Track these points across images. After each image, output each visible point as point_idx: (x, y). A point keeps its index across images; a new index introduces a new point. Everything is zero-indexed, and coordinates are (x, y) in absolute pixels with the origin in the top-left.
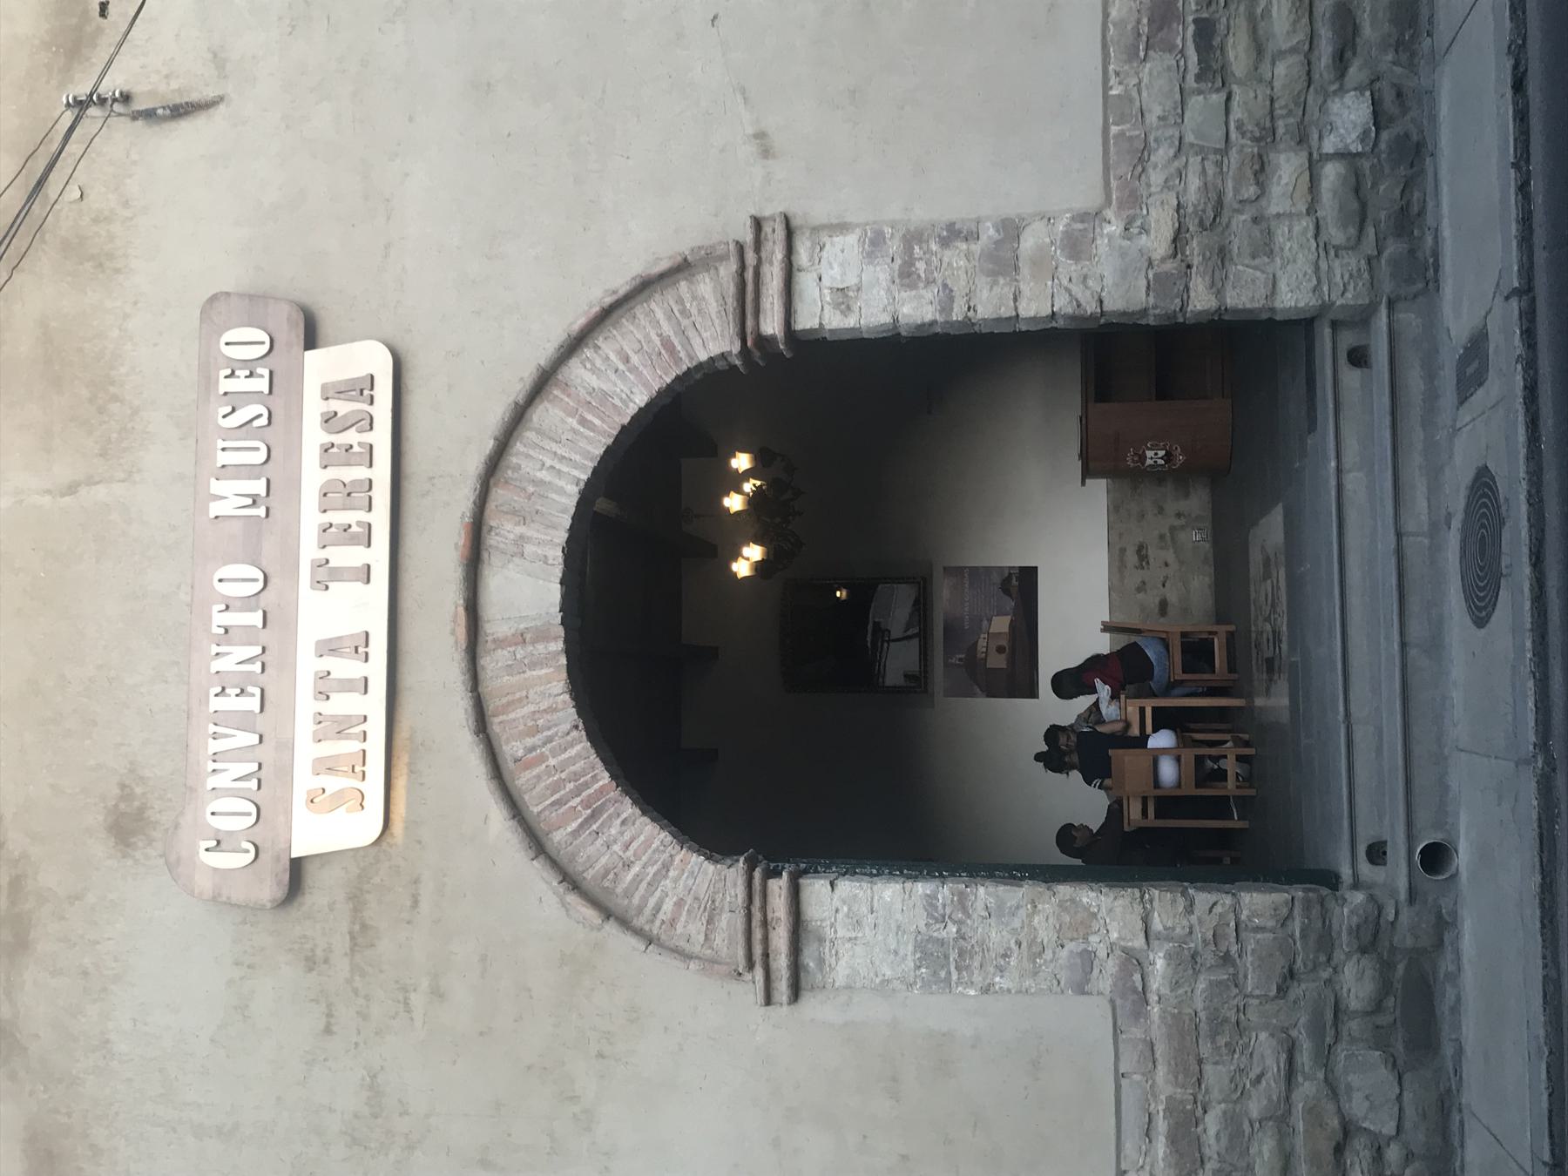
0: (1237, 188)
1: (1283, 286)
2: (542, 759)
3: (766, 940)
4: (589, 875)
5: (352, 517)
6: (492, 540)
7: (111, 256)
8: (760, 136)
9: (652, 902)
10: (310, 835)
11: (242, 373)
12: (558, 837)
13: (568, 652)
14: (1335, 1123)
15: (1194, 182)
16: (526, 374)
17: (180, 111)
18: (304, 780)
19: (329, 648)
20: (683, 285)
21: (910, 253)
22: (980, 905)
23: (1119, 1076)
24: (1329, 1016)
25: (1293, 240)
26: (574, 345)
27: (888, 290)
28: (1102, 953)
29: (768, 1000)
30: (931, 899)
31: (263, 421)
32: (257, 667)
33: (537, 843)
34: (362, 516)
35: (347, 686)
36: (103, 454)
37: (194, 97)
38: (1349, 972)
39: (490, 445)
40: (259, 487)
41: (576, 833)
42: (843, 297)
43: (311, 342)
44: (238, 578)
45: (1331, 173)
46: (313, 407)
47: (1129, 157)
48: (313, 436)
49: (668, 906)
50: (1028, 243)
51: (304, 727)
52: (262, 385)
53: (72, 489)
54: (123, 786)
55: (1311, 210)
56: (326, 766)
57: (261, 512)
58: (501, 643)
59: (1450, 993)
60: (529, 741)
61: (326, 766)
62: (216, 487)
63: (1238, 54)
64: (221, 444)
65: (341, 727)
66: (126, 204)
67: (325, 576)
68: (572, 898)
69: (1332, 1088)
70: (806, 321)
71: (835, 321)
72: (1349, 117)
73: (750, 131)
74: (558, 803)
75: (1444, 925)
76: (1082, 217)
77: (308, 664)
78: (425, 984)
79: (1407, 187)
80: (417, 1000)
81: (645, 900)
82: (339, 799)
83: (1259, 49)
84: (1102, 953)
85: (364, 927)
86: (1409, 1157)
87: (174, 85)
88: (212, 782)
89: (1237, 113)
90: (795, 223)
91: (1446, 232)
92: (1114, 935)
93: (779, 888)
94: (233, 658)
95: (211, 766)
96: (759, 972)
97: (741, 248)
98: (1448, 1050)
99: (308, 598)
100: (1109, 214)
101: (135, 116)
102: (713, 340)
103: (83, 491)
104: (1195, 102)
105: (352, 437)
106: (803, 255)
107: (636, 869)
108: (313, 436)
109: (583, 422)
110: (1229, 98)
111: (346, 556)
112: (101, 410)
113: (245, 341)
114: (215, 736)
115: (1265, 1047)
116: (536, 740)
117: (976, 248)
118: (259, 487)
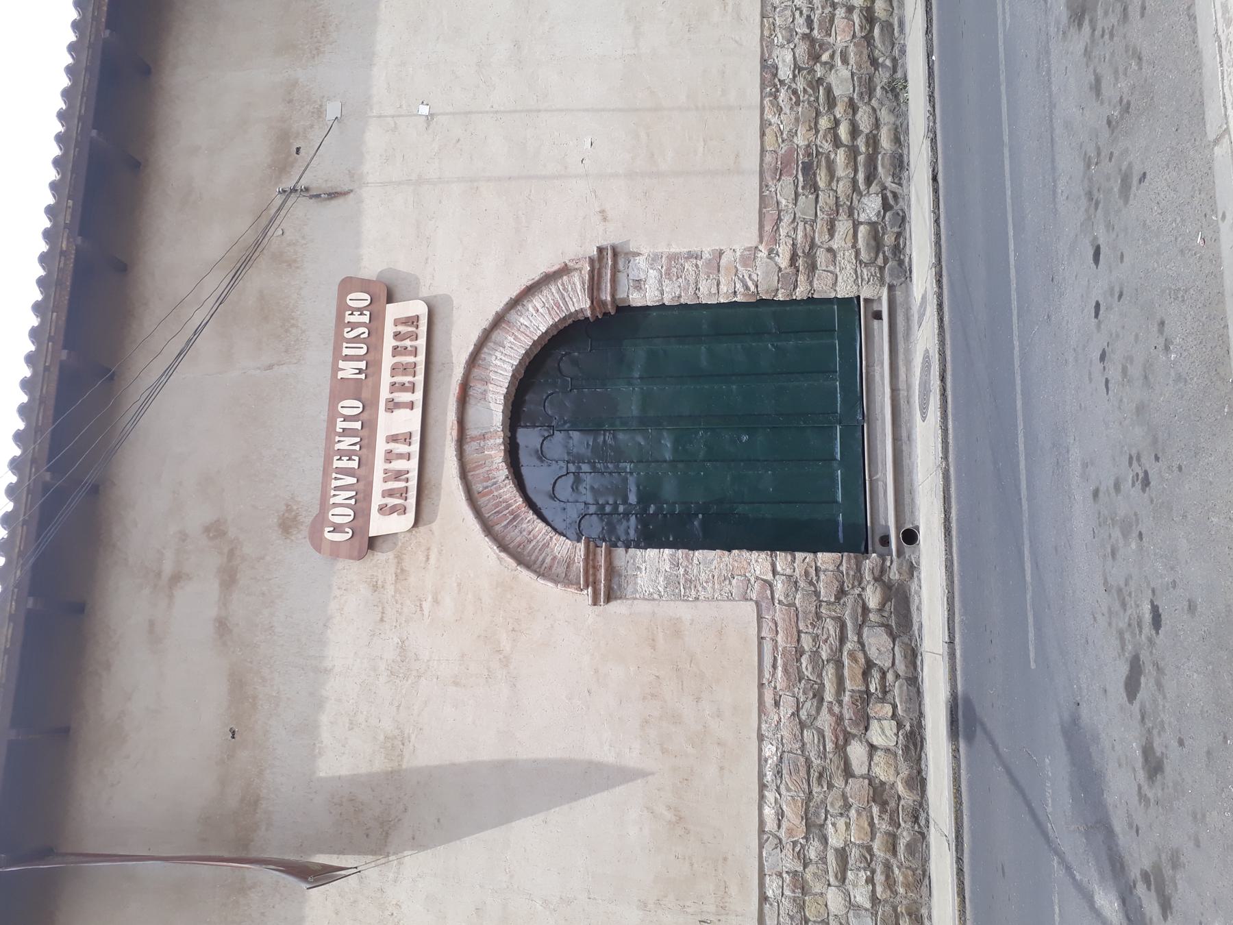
0: (821, 237)
1: (840, 279)
2: (491, 492)
3: (594, 575)
4: (511, 546)
5: (407, 379)
6: (471, 392)
7: (295, 261)
8: (602, 212)
9: (541, 558)
10: (379, 525)
11: (356, 313)
12: (498, 528)
13: (504, 443)
14: (862, 661)
15: (800, 234)
16: (490, 316)
17: (333, 195)
18: (377, 500)
19: (394, 439)
20: (565, 278)
21: (673, 264)
22: (695, 561)
23: (761, 639)
24: (860, 610)
25: (846, 259)
26: (515, 303)
27: (660, 282)
28: (752, 580)
29: (595, 603)
30: (673, 555)
31: (366, 335)
32: (357, 448)
34: (410, 378)
35: (400, 456)
36: (286, 351)
37: (339, 190)
38: (869, 589)
39: (471, 348)
40: (362, 365)
41: (506, 527)
43: (390, 300)
44: (351, 406)
46: (389, 329)
49: (548, 560)
51: (378, 475)
52: (366, 319)
53: (270, 367)
54: (287, 506)
55: (854, 246)
56: (390, 493)
57: (363, 376)
58: (473, 439)
59: (917, 601)
60: (485, 484)
61: (390, 493)
62: (342, 364)
64: (345, 345)
65: (398, 475)
66: (303, 237)
67: (393, 406)
68: (503, 555)
72: (871, 206)
73: (598, 209)
74: (498, 512)
75: (912, 569)
76: (749, 249)
77: (381, 446)
78: (430, 599)
79: (899, 235)
80: (426, 606)
81: (537, 558)
82: (393, 510)
84: (752, 580)
85: (402, 570)
86: (897, 676)
87: (329, 184)
88: (332, 501)
89: (820, 204)
90: (618, 250)
91: (914, 255)
92: (758, 573)
93: (602, 550)
94: (346, 443)
95: (333, 492)
96: (590, 589)
97: (592, 261)
98: (915, 627)
100: (761, 247)
101: (311, 197)
102: (580, 303)
103: (276, 367)
104: (802, 199)
105: (408, 343)
106: (621, 265)
107: (534, 543)
108: (389, 342)
109: (516, 338)
110: (817, 197)
111: (405, 397)
112: (287, 331)
113: (359, 299)
114: (336, 479)
115: (831, 627)
116: (489, 483)
117: (700, 263)
118: (362, 365)
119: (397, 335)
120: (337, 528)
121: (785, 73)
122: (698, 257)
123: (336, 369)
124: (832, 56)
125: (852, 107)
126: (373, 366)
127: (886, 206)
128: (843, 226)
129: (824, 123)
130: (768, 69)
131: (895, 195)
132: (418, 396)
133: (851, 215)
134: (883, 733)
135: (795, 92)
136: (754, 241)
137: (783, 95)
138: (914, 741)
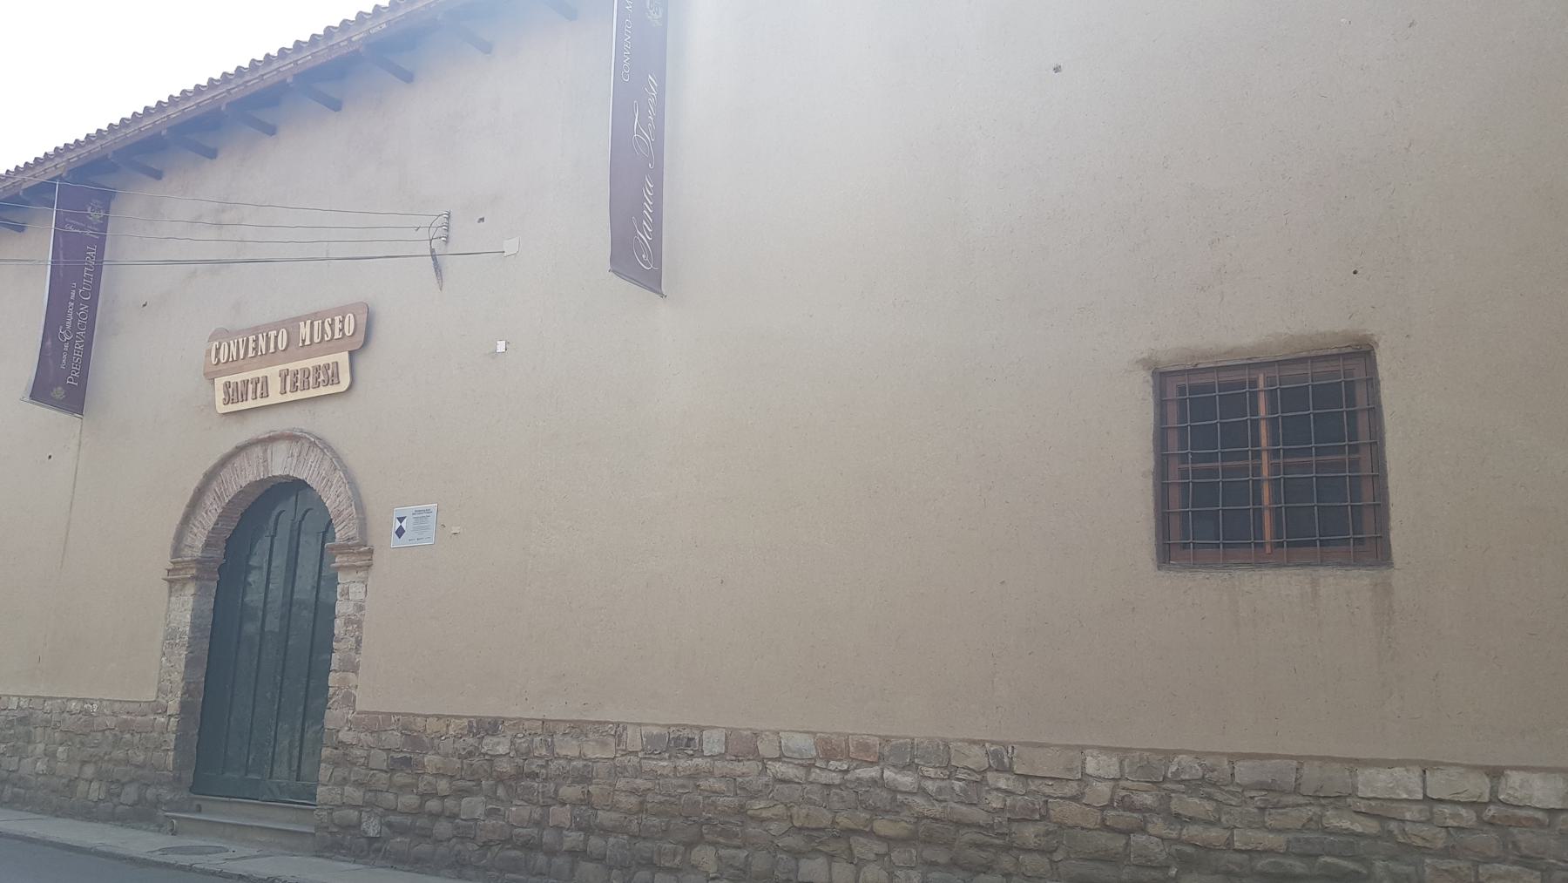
10: (220, 382)
17: (438, 269)
18: (233, 378)
33: (210, 476)
42: (346, 593)
43: (351, 353)
47: (375, 723)
48: (321, 361)
50: (351, 675)
63: (400, 778)
67: (284, 376)
69: (132, 781)
70: (341, 577)
71: (339, 588)
72: (372, 827)
77: (260, 373)
83: (402, 788)
94: (262, 343)
99: (278, 368)
102: (341, 533)
104: (384, 755)
119: (327, 367)
120: (218, 350)
121: (489, 744)
124: (498, 799)
126: (310, 350)
127: (371, 840)
128: (356, 795)
129: (443, 785)
130: (491, 727)
131: (379, 850)
132: (290, 397)
133: (367, 804)
134: (96, 791)
137: (470, 740)
138: (88, 813)
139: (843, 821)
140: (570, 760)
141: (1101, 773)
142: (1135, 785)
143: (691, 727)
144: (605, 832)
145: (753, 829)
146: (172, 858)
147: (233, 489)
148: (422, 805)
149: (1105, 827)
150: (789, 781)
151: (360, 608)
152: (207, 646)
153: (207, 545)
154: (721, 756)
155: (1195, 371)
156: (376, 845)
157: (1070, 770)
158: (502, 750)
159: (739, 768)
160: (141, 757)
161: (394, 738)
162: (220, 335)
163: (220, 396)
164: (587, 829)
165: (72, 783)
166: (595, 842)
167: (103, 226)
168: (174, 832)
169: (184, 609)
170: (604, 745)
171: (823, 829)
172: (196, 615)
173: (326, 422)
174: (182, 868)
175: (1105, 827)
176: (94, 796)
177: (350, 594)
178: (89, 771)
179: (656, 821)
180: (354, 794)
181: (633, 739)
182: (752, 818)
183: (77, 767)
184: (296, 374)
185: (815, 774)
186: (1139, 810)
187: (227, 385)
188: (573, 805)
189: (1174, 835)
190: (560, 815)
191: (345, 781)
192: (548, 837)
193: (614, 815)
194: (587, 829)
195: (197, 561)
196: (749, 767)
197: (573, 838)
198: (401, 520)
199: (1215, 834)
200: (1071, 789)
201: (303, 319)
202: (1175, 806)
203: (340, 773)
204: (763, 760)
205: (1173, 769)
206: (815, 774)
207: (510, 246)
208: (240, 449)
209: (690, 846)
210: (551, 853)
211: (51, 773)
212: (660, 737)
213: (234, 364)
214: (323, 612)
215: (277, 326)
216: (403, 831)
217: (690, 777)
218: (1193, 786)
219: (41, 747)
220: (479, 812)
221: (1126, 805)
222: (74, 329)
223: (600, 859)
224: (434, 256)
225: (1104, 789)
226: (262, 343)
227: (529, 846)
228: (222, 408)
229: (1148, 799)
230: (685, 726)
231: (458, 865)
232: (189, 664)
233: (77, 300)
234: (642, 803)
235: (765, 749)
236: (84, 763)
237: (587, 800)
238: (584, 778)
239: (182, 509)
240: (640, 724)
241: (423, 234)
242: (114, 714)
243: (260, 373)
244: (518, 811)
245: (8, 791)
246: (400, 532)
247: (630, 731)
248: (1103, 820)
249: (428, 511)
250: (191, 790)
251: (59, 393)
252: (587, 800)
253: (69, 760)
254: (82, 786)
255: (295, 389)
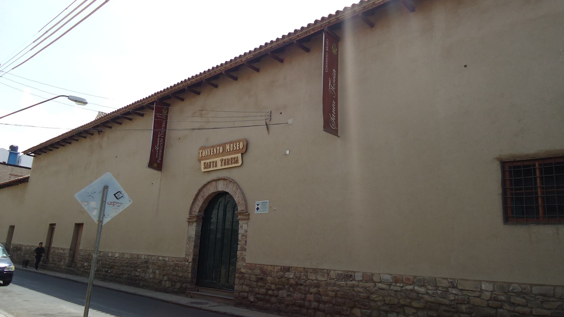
10: (203, 162)
33: (200, 191)
42: (242, 227)
43: (242, 154)
45: (246, 294)
47: (252, 267)
48: (233, 156)
50: (244, 252)
63: (260, 284)
65: (210, 166)
67: (222, 160)
69: (178, 281)
70: (240, 222)
72: (252, 299)
77: (214, 160)
83: (261, 287)
94: (215, 151)
102: (240, 208)
108: (233, 156)
119: (235, 158)
121: (287, 274)
122: (246, 244)
123: (227, 143)
124: (291, 292)
125: (276, 296)
126: (229, 153)
127: (252, 302)
128: (246, 288)
129: (273, 287)
130: (288, 269)
132: (224, 167)
133: (250, 291)
134: (168, 284)
135: (281, 277)
136: (247, 261)
137: (281, 273)
138: (165, 291)
139: (402, 302)
140: (313, 280)
141: (487, 289)
142: (499, 293)
143: (351, 272)
144: (325, 303)
145: (372, 304)
146: (190, 305)
147: (207, 194)
148: (267, 292)
149: (488, 306)
150: (384, 289)
151: (246, 232)
152: (199, 242)
153: (200, 211)
154: (361, 281)
155: (515, 161)
156: (253, 304)
157: (476, 288)
158: (291, 276)
159: (367, 285)
160: (181, 274)
161: (258, 271)
162: (203, 148)
163: (203, 166)
164: (319, 302)
165: (160, 282)
166: (321, 306)
167: (167, 117)
168: (191, 297)
169: (193, 230)
170: (323, 276)
171: (395, 305)
172: (197, 232)
173: (234, 175)
174: (198, 308)
175: (488, 306)
176: (167, 285)
177: (243, 227)
178: (166, 278)
179: (341, 300)
180: (246, 288)
181: (333, 274)
182: (372, 300)
183: (162, 277)
184: (225, 160)
185: (392, 287)
186: (500, 301)
187: (205, 163)
188: (314, 294)
189: (512, 309)
190: (310, 297)
191: (243, 284)
192: (307, 304)
193: (327, 298)
194: (319, 302)
195: (197, 216)
196: (370, 284)
197: (315, 304)
198: (258, 205)
199: (526, 310)
200: (477, 294)
201: (227, 143)
202: (512, 300)
203: (242, 281)
204: (375, 282)
205: (511, 288)
206: (392, 287)
207: (290, 121)
208: (209, 183)
209: (352, 308)
210: (308, 308)
211: (154, 278)
212: (341, 274)
213: (207, 157)
214: (234, 232)
215: (219, 146)
216: (261, 300)
217: (352, 287)
218: (518, 294)
219: (151, 270)
220: (285, 295)
221: (496, 300)
222: (160, 146)
223: (323, 311)
224: (267, 125)
225: (488, 294)
226: (215, 151)
227: (301, 306)
228: (203, 170)
229: (503, 298)
230: (349, 271)
231: (279, 311)
232: (195, 247)
233: (160, 137)
234: (336, 294)
235: (375, 279)
236: (164, 275)
237: (318, 293)
238: (317, 286)
239: (192, 200)
240: (335, 270)
241: (263, 118)
242: (173, 261)
243: (214, 160)
244: (297, 295)
245: (142, 283)
246: (258, 209)
247: (332, 272)
248: (488, 304)
249: (266, 202)
250: (196, 285)
251: (155, 165)
252: (318, 293)
253: (160, 274)
254: (163, 283)
255: (225, 165)
